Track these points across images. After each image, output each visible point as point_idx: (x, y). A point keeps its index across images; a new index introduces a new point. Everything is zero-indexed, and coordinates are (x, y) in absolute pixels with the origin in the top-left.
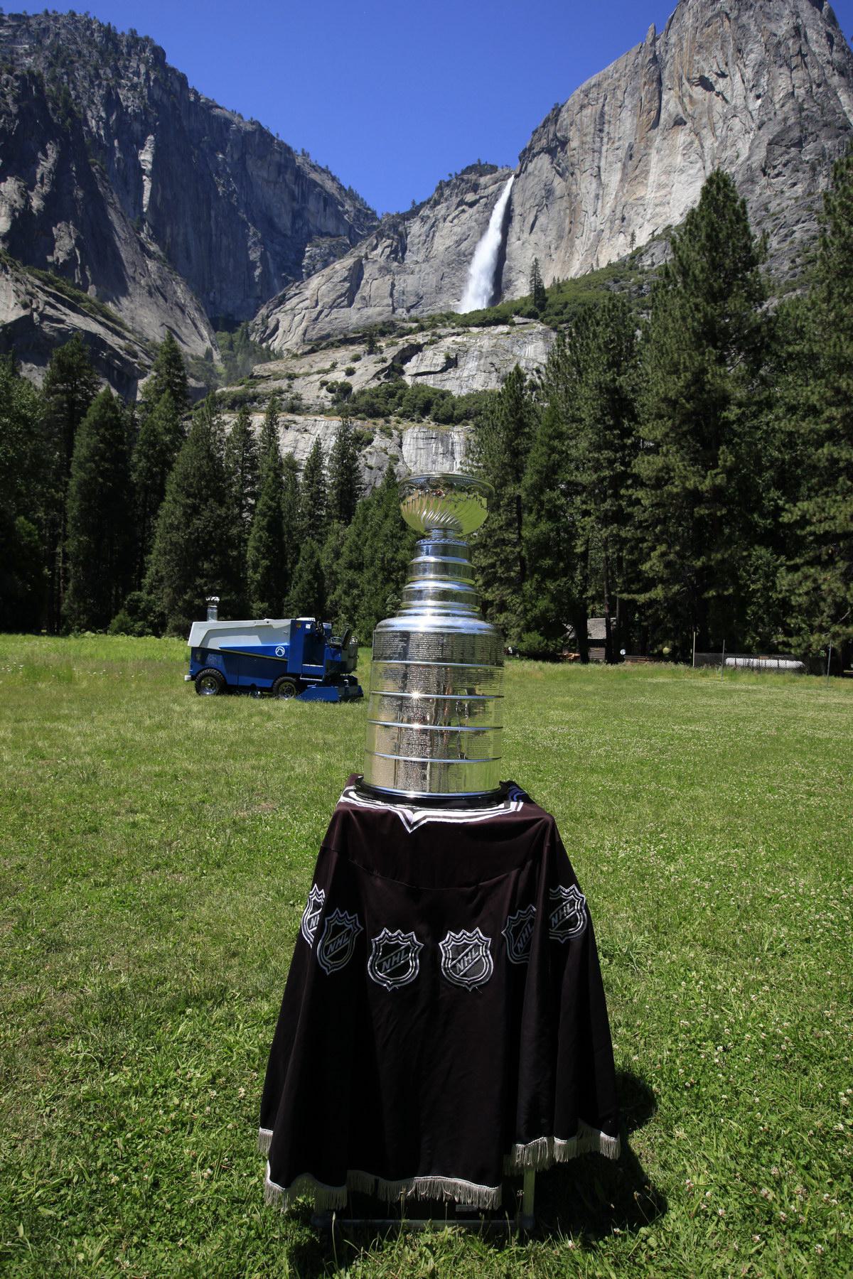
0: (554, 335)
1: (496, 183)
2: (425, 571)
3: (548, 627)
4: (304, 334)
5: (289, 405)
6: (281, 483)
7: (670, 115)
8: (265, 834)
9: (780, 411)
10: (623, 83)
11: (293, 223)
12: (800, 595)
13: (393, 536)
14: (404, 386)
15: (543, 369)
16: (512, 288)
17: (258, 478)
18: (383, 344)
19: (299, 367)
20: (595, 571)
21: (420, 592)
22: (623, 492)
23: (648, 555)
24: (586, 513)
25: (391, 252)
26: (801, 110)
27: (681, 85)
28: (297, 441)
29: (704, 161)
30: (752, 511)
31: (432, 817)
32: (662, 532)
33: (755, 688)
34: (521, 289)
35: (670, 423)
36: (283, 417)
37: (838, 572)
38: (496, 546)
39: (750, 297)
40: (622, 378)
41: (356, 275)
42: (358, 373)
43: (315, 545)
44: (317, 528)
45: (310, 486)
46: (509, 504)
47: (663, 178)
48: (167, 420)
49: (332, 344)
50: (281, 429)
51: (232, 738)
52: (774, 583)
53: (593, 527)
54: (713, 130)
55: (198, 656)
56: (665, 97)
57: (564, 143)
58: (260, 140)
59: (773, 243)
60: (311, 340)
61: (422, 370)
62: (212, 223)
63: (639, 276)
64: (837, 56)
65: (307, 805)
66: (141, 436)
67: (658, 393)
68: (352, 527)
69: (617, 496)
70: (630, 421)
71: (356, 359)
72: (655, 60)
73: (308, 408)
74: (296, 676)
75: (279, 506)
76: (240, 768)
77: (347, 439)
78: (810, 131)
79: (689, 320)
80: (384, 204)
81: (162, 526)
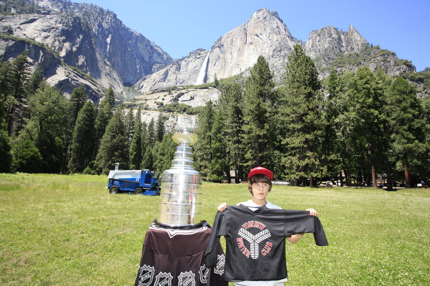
0: (220, 92)
2: (179, 155)
3: (219, 173)
4: (151, 88)
5: (145, 108)
8: (128, 239)
9: (280, 115)
10: (237, 33)
11: (149, 59)
12: (287, 164)
13: (174, 146)
14: (178, 104)
15: (217, 101)
17: (134, 128)
19: (148, 97)
20: (232, 157)
21: (177, 162)
22: (239, 135)
23: (247, 152)
24: (229, 141)
25: (176, 69)
26: (280, 44)
27: (251, 35)
28: (147, 118)
30: (274, 141)
31: (178, 233)
32: (250, 146)
33: (277, 190)
34: (211, 80)
35: (252, 116)
37: (297, 157)
38: (204, 149)
39: (270, 86)
40: (239, 104)
42: (165, 100)
43: (150, 148)
44: (151, 143)
45: (150, 131)
46: (208, 138)
47: (248, 56)
49: (159, 92)
50: (142, 114)
51: (120, 207)
52: (281, 161)
54: (260, 46)
55: (111, 181)
57: (223, 46)
58: (142, 38)
59: (275, 73)
64: (287, 33)
65: (142, 229)
66: (99, 114)
67: (248, 109)
68: (162, 143)
69: (238, 136)
70: (241, 116)
71: (165, 96)
72: (245, 29)
74: (142, 188)
75: (140, 136)
76: (121, 218)
79: (256, 90)
80: (175, 56)
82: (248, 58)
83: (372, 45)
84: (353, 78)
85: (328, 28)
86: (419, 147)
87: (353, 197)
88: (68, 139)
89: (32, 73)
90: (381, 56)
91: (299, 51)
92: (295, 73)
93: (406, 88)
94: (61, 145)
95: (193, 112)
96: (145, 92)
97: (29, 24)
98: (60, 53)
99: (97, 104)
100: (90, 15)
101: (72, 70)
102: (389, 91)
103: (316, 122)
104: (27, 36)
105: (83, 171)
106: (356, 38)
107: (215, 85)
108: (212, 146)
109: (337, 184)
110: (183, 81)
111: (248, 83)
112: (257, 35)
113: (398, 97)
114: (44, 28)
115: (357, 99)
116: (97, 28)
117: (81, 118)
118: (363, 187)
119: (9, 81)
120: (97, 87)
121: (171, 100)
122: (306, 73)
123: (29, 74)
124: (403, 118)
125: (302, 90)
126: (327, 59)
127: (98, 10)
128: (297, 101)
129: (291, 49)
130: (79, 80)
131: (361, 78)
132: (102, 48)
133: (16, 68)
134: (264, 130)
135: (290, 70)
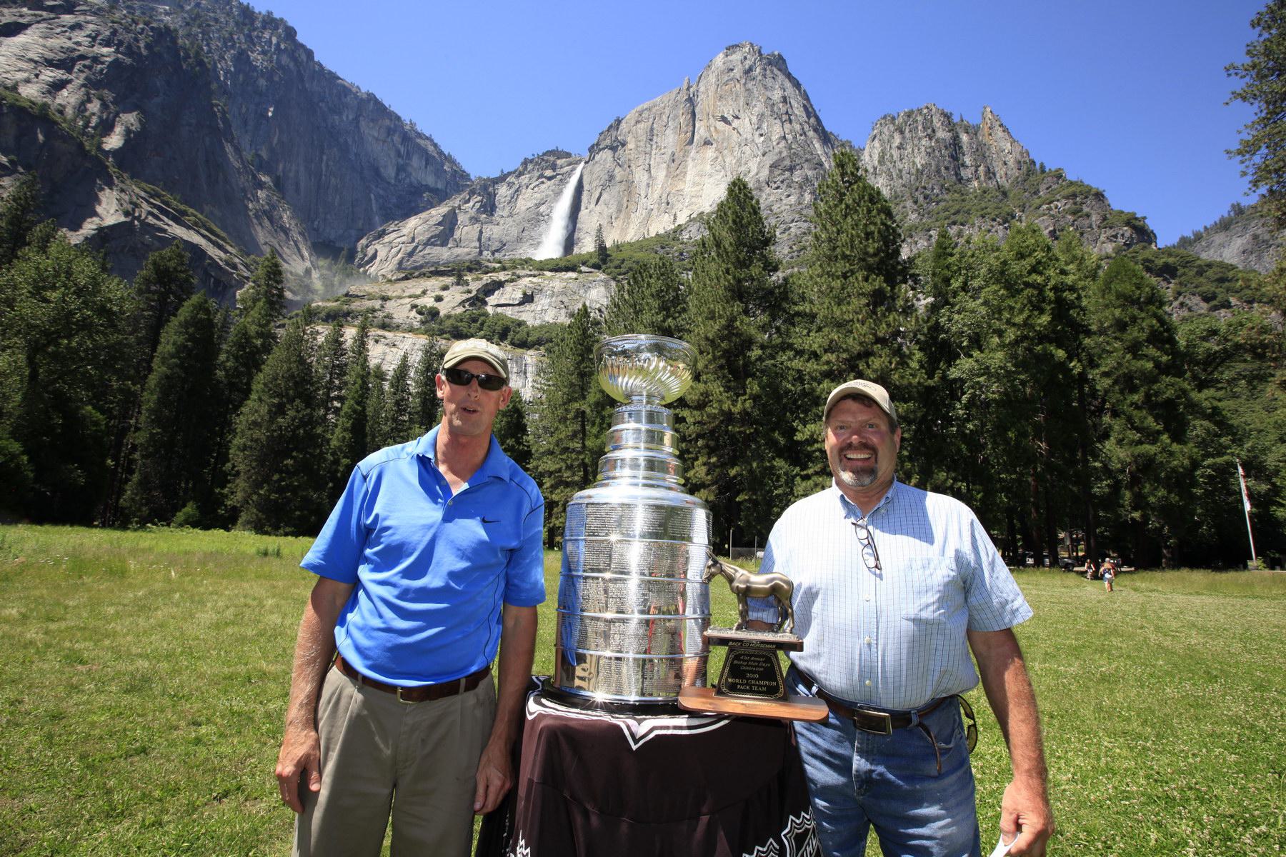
0: (613, 284)
4: (400, 263)
6: (368, 389)
9: (792, 353)
10: (667, 111)
14: (486, 315)
15: (604, 309)
17: (346, 383)
19: (392, 291)
23: (693, 464)
25: (481, 207)
26: (790, 148)
28: (385, 354)
29: (726, 171)
30: (773, 430)
34: (587, 246)
35: (710, 356)
36: (374, 332)
40: (670, 320)
41: (449, 223)
42: (446, 300)
45: (395, 394)
46: (576, 417)
48: (260, 325)
49: (424, 274)
50: (370, 344)
52: (792, 489)
54: (732, 151)
56: (697, 125)
57: (623, 145)
58: (374, 108)
59: (777, 234)
60: (405, 269)
61: (502, 302)
64: (812, 120)
67: (699, 334)
71: (445, 288)
72: (690, 100)
73: (398, 326)
75: (364, 409)
77: (432, 354)
78: (797, 161)
80: (477, 166)
81: (244, 423)
82: (698, 184)
83: (1042, 167)
86: (1171, 454)
88: (125, 416)
90: (1067, 198)
91: (849, 169)
93: (1138, 288)
95: (529, 339)
96: (382, 272)
98: (104, 139)
99: (224, 306)
100: (209, 25)
101: (143, 194)
102: (1095, 294)
106: (1002, 144)
108: (589, 443)
110: (500, 245)
111: (699, 258)
112: (724, 119)
113: (1117, 312)
114: (50, 55)
116: (232, 69)
120: (226, 252)
121: (463, 301)
122: (868, 235)
124: (1130, 371)
125: (856, 285)
126: (921, 198)
127: (236, 13)
128: (843, 313)
129: (821, 165)
130: (166, 227)
131: (1021, 256)
132: (246, 132)
135: (823, 225)
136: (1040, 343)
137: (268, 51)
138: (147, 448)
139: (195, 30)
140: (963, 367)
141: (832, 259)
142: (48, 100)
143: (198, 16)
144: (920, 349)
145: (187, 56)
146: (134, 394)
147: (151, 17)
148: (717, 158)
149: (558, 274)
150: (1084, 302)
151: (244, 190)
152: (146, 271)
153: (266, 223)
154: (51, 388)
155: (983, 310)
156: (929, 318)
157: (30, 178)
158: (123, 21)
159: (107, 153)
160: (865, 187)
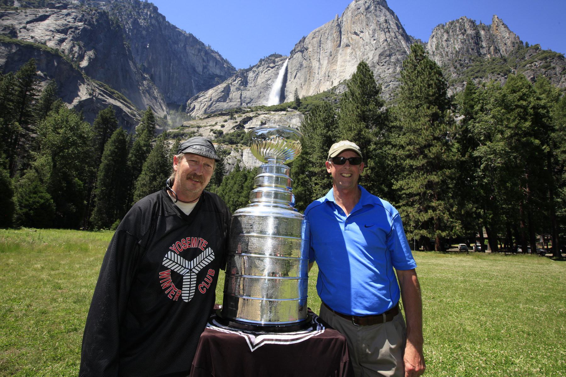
0: (303, 116)
1: (281, 61)
4: (205, 111)
7: (344, 43)
10: (327, 32)
13: (238, 192)
14: (244, 133)
15: (299, 128)
16: (287, 98)
18: (237, 116)
19: (202, 123)
24: (316, 184)
25: (241, 83)
26: (389, 45)
29: (357, 59)
30: (382, 184)
34: (290, 99)
37: (416, 209)
41: (227, 91)
42: (226, 127)
47: (343, 63)
48: (145, 141)
49: (216, 115)
53: (319, 189)
56: (342, 37)
57: (307, 49)
58: (192, 40)
59: (383, 87)
60: (207, 113)
62: (171, 68)
63: (335, 96)
64: (401, 30)
68: (220, 187)
71: (226, 121)
72: (339, 25)
79: (355, 112)
80: (239, 64)
82: (344, 66)
83: (527, 44)
84: (499, 91)
85: (461, 21)
87: (504, 268)
88: (91, 182)
89: (42, 90)
90: (541, 60)
92: (414, 85)
94: (81, 189)
97: (39, 22)
98: (81, 63)
99: (131, 133)
100: (121, 9)
101: (96, 86)
102: (557, 110)
103: (444, 156)
104: (36, 39)
105: (112, 227)
106: (504, 34)
107: (295, 105)
109: (474, 247)
110: (250, 100)
114: (58, 28)
115: (507, 123)
117: (108, 152)
118: (515, 253)
119: (12, 101)
120: (131, 109)
121: (234, 127)
122: (429, 86)
123: (40, 91)
125: (423, 111)
126: (458, 66)
128: (416, 126)
129: (405, 52)
130: (106, 99)
131: (514, 91)
133: (21, 83)
134: (366, 169)
135: (405, 82)
136: (525, 136)
137: (146, 18)
138: (100, 196)
139: (116, 11)
140: (481, 151)
141: (411, 99)
142: (58, 47)
143: (117, 5)
144: (458, 142)
145: (113, 23)
146: (95, 173)
147: (98, 7)
148: (352, 53)
149: (277, 113)
150: (551, 114)
151: (138, 81)
152: (98, 119)
153: (147, 95)
154: (61, 171)
155: (492, 121)
156: (462, 126)
157: (52, 81)
158: (87, 10)
159: (82, 69)
160: (427, 62)
